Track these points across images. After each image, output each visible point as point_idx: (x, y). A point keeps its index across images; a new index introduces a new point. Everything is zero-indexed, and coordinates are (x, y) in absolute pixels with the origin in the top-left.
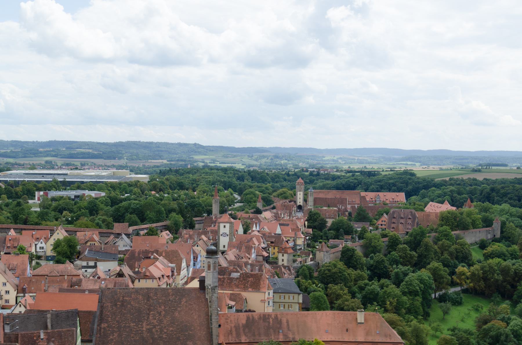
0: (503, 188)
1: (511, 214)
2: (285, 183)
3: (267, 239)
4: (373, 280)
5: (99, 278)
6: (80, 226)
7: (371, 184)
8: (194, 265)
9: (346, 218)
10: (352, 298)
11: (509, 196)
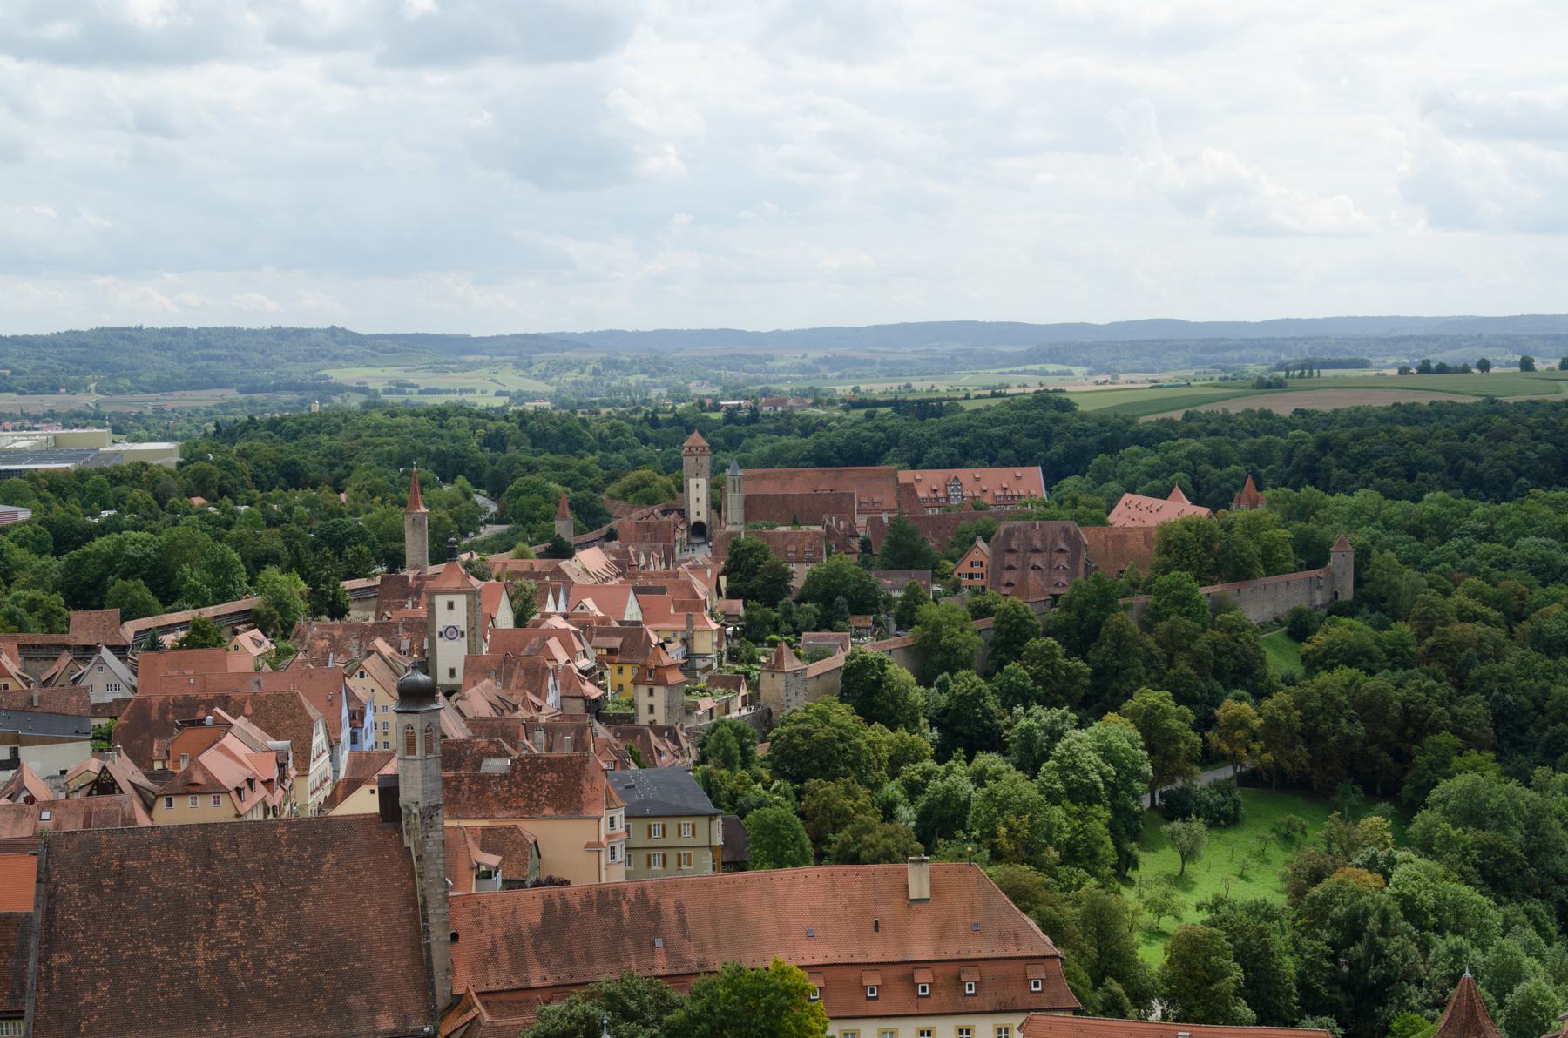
0: (1356, 438)
1: (1385, 522)
2: (643, 451)
3: (597, 640)
4: (949, 757)
5: (30, 800)
7: (931, 443)
8: (354, 739)
9: (854, 558)
11: (1377, 463)
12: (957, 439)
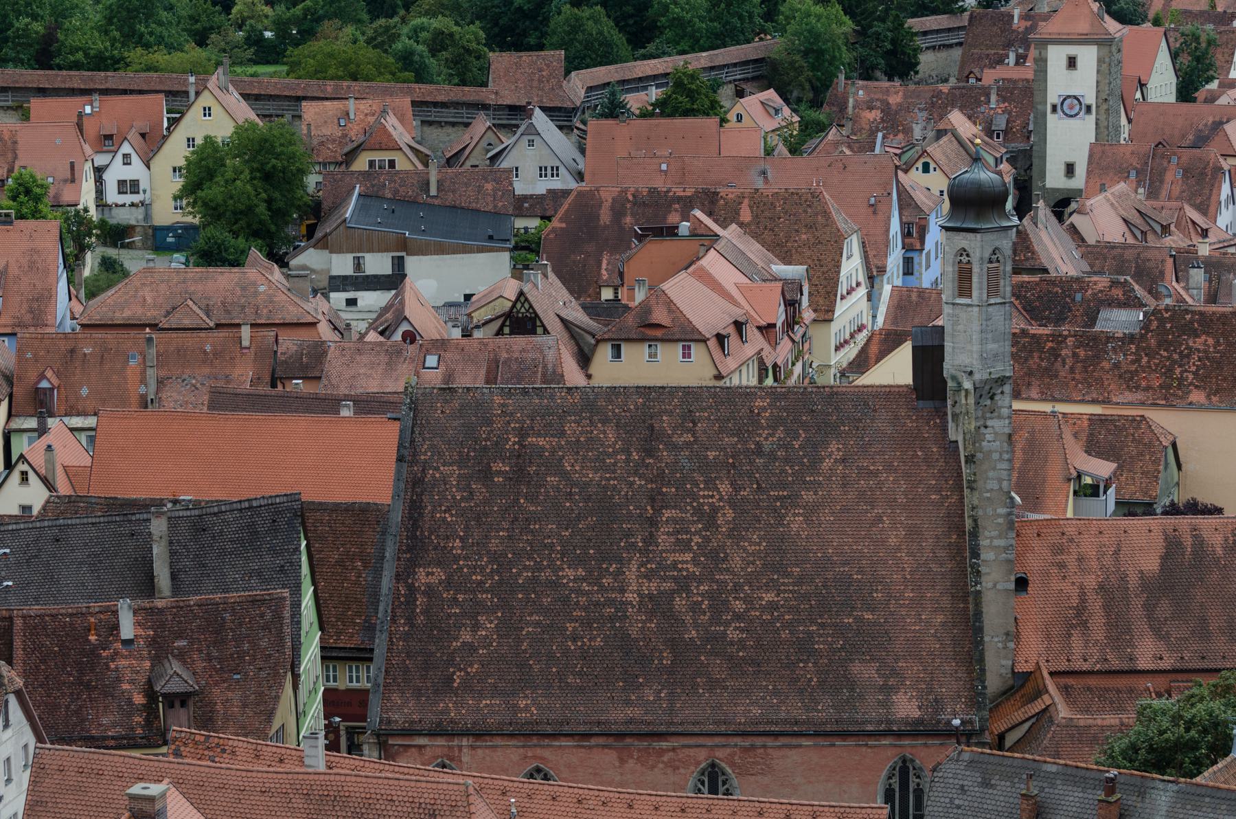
5: (410, 337)
6: (319, 73)
8: (908, 268)
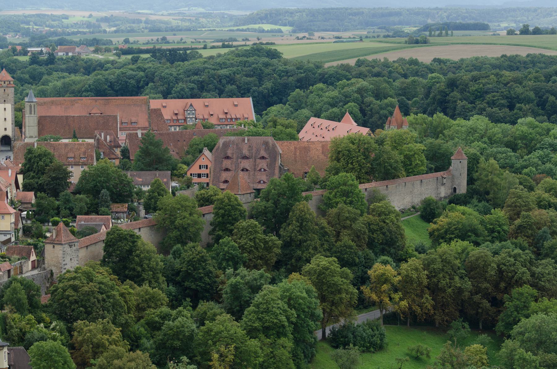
0: (475, 79)
1: (490, 139)
9: (117, 162)
10: (130, 350)
11: (489, 97)
12: (196, 77)
